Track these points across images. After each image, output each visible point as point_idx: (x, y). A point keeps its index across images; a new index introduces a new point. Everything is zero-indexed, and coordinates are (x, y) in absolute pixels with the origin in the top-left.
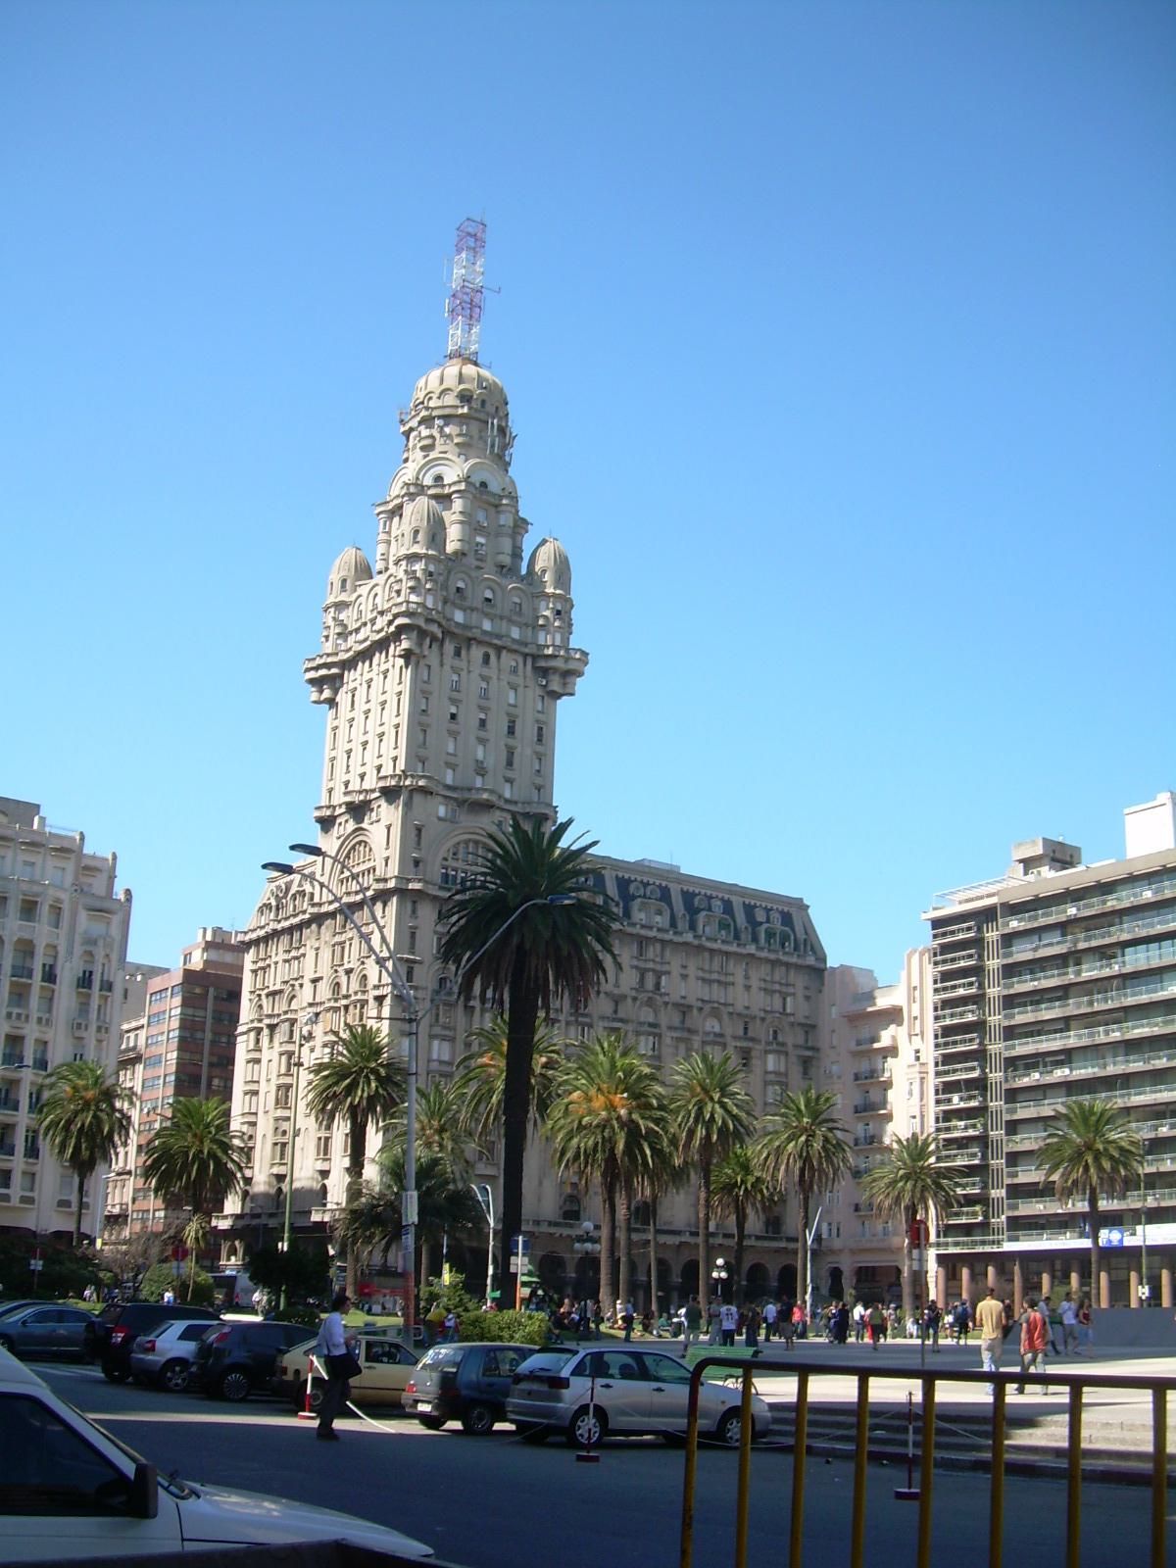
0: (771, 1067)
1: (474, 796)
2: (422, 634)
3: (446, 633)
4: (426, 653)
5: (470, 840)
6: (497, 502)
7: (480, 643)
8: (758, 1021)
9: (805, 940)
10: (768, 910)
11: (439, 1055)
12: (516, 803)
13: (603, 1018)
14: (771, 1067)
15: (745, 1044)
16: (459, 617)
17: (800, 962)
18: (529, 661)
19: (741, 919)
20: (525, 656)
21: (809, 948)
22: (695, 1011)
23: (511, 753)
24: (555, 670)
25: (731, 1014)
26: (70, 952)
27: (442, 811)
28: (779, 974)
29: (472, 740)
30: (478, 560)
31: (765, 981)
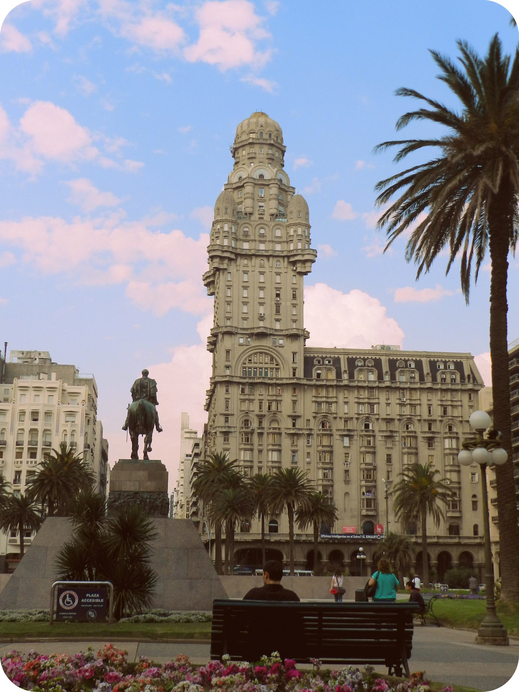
0: (447, 446)
1: (256, 331)
2: (222, 258)
3: (237, 255)
4: (225, 266)
5: (257, 352)
6: (267, 183)
7: (257, 256)
8: (438, 422)
9: (469, 376)
10: (445, 363)
11: (244, 458)
12: (282, 330)
13: (338, 430)
14: (447, 446)
15: (431, 435)
16: (246, 246)
17: (464, 388)
18: (286, 259)
19: (426, 369)
20: (283, 257)
21: (471, 380)
22: (396, 421)
23: (278, 306)
24: (299, 261)
25: (419, 420)
26: (57, 431)
27: (241, 341)
28: (448, 396)
29: (256, 303)
30: (260, 214)
31: (441, 401)
